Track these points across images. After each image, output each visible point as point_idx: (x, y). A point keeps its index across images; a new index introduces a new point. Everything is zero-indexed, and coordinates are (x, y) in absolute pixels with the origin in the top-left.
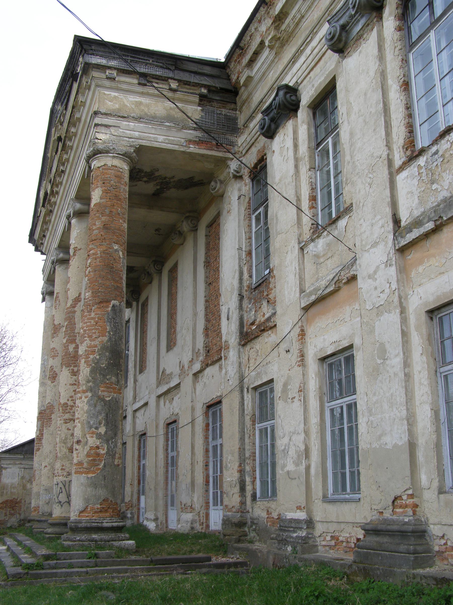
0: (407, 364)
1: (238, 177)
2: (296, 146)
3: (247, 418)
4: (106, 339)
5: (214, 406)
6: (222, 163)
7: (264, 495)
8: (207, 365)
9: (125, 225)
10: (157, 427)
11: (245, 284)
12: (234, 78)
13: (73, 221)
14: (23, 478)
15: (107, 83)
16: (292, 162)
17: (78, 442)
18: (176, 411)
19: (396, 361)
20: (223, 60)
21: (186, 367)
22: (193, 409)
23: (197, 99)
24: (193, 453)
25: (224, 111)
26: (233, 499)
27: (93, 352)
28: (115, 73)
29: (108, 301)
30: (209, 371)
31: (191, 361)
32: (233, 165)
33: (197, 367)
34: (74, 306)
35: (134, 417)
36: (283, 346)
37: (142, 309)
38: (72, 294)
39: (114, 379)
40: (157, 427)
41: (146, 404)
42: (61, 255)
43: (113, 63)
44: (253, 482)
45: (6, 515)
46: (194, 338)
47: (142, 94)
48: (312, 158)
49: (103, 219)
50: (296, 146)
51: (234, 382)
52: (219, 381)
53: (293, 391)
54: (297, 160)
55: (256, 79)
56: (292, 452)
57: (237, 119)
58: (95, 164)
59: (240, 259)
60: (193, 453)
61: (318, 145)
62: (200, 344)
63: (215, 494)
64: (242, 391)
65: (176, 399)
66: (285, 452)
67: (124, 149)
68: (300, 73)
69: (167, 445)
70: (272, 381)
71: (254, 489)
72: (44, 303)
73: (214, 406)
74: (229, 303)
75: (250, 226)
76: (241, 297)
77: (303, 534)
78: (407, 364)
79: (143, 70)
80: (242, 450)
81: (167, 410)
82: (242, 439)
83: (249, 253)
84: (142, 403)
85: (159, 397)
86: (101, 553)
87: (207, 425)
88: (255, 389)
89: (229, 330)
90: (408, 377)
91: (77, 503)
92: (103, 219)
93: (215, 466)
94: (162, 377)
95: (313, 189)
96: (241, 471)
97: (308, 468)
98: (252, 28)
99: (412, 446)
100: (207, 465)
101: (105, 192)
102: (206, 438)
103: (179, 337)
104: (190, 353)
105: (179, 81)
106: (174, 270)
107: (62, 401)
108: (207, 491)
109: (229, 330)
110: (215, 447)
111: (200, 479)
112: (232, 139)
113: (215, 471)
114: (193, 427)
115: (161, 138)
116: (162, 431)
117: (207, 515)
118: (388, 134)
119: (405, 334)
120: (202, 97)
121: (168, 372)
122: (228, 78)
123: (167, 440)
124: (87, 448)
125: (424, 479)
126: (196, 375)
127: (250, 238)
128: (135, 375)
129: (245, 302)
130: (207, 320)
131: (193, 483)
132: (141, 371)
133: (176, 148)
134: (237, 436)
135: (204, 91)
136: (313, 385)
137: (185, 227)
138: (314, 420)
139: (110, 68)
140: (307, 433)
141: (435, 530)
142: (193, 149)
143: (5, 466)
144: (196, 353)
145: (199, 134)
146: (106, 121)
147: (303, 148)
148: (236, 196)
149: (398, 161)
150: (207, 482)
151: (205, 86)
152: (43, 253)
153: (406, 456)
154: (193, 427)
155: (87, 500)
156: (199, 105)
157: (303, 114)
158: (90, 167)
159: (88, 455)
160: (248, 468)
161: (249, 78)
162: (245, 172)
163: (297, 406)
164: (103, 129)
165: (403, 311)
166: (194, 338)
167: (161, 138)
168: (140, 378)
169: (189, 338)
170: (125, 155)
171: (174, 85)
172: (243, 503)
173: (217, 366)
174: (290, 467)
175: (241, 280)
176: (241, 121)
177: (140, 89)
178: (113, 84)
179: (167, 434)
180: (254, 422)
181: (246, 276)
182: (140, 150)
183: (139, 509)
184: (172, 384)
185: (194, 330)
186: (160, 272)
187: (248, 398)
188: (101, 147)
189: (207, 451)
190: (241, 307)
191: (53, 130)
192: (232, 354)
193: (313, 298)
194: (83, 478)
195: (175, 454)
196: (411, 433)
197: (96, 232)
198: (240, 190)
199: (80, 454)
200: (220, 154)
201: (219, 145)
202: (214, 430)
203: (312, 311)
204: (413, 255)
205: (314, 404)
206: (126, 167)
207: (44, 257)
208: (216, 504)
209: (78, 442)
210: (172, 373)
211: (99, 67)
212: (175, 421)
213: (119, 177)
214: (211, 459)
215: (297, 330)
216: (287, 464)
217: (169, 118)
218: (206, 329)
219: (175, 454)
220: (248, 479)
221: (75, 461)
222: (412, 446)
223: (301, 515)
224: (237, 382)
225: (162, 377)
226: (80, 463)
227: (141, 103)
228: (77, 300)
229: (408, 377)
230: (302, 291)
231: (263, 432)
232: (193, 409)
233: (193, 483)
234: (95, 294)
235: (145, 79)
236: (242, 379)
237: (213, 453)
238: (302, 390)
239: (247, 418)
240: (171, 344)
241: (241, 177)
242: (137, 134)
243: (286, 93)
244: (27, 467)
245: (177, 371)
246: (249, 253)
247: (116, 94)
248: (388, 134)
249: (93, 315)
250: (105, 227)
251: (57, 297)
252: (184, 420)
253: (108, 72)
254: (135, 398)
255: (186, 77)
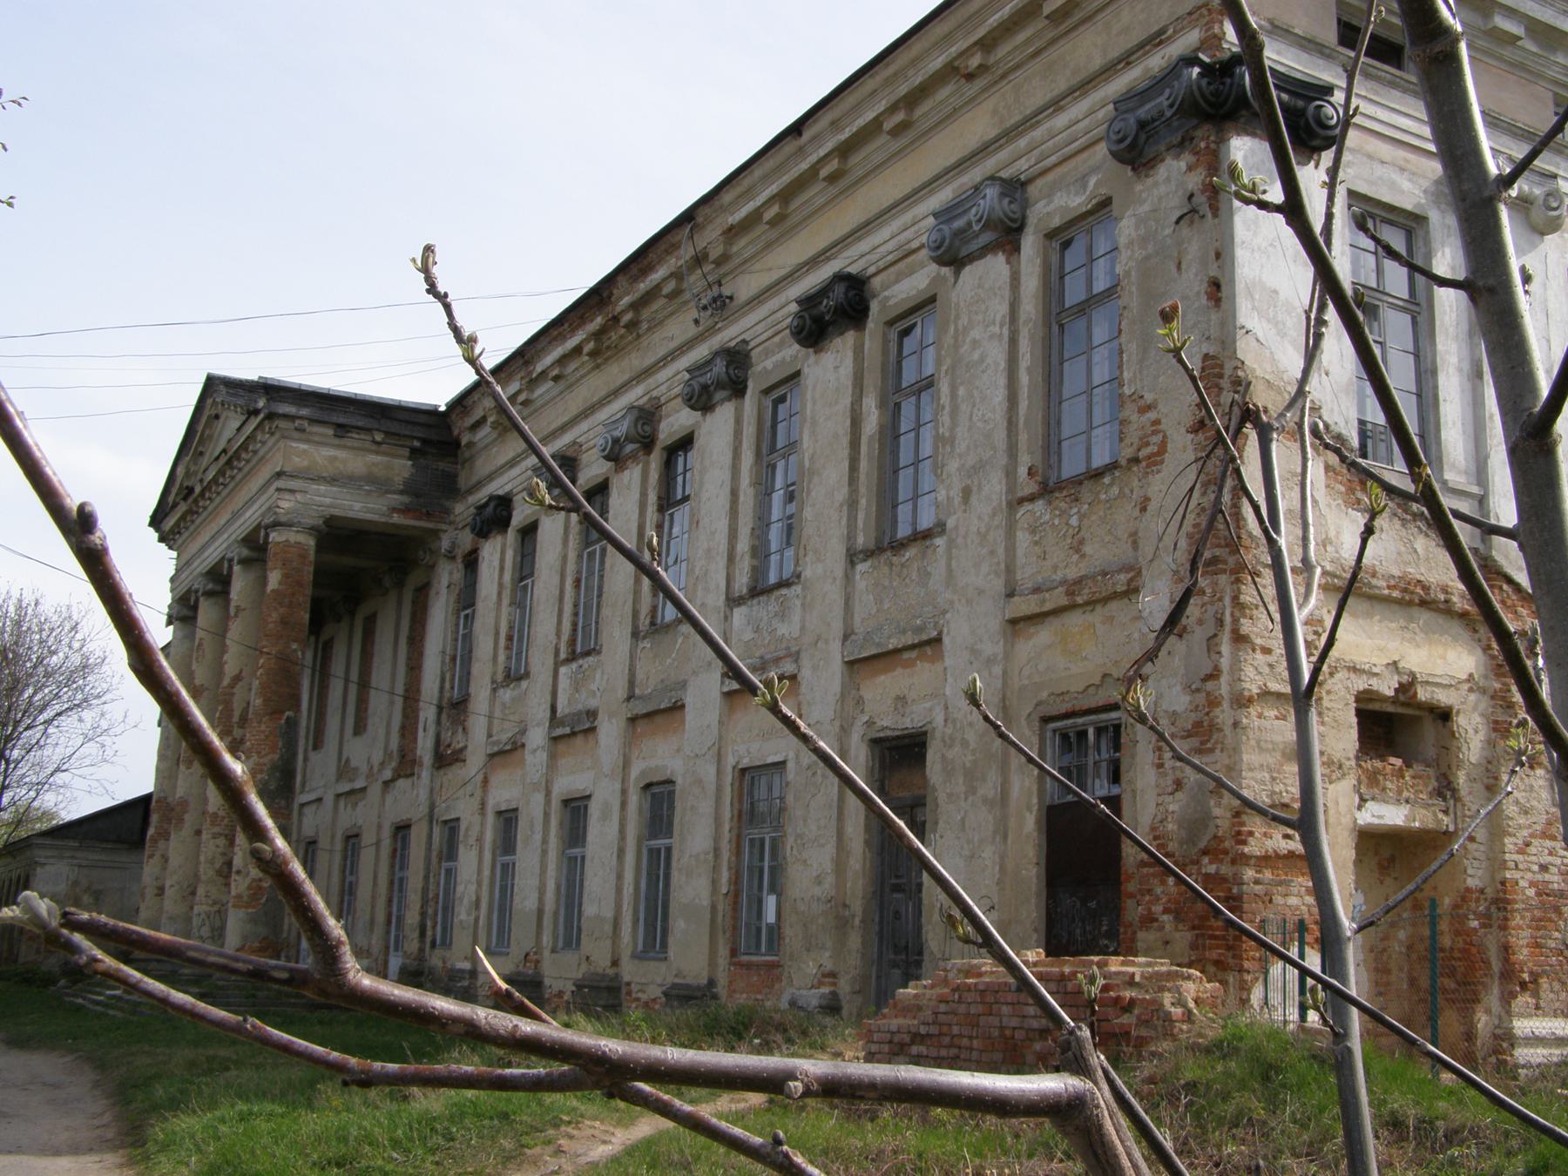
0: (545, 841)
1: (451, 557)
2: (502, 569)
3: (434, 854)
4: (277, 757)
5: (402, 829)
6: (436, 534)
7: (443, 943)
8: (399, 776)
9: (307, 616)
10: (333, 837)
11: (447, 695)
12: (456, 433)
13: (236, 568)
14: (76, 883)
15: (296, 435)
16: (495, 586)
17: (238, 872)
18: (360, 822)
19: (538, 837)
20: (443, 408)
21: (375, 769)
22: (380, 826)
23: (406, 452)
24: (375, 884)
25: (442, 465)
26: (412, 946)
27: (261, 771)
28: (306, 423)
29: (282, 712)
30: (401, 783)
31: (382, 764)
32: (445, 544)
33: (388, 774)
34: (232, 685)
35: (300, 814)
36: (469, 788)
37: (324, 649)
38: (230, 669)
39: (283, 803)
40: (333, 837)
41: (319, 800)
42: (210, 586)
43: (304, 412)
44: (434, 927)
45: (38, 952)
46: (388, 733)
47: (338, 447)
48: (513, 591)
49: (282, 610)
50: (502, 569)
51: (423, 810)
52: (410, 799)
53: (472, 841)
54: (501, 585)
55: (480, 445)
56: (465, 901)
57: (456, 476)
58: (274, 536)
59: (443, 662)
60: (375, 884)
61: (522, 579)
62: (394, 744)
63: (397, 937)
64: (431, 822)
65: (360, 805)
66: (461, 899)
67: (310, 522)
68: (515, 482)
69: (345, 866)
70: (458, 819)
71: (434, 935)
72: (171, 628)
73: (402, 830)
74: (428, 713)
75: (457, 625)
76: (440, 708)
77: (466, 983)
78: (545, 841)
79: (341, 420)
80: (425, 890)
81: (349, 817)
82: (426, 878)
83: (454, 659)
84: (312, 797)
85: (338, 796)
86: (260, 994)
87: (395, 851)
88: (445, 822)
89: (424, 745)
90: (544, 852)
91: (232, 940)
92: (282, 610)
93: (400, 902)
94: (345, 770)
95: (511, 628)
96: (423, 914)
97: (477, 920)
98: (476, 396)
99: (540, 912)
100: (390, 901)
101: (286, 576)
102: (392, 866)
103: (370, 722)
104: (381, 753)
105: (387, 433)
106: (371, 621)
107: (211, 808)
108: (388, 932)
109: (424, 745)
110: (401, 880)
111: (381, 917)
112: (447, 504)
113: (399, 910)
114: (378, 850)
115: (358, 506)
116: (339, 846)
117: (386, 962)
118: (559, 622)
119: (546, 815)
120: (414, 451)
121: (353, 763)
122: (449, 428)
123: (345, 858)
124: (248, 881)
125: (545, 939)
126: (387, 784)
127: (456, 640)
128: (306, 751)
129: (444, 716)
130: (405, 716)
131: (372, 922)
132: (316, 747)
133: (376, 518)
134: (422, 873)
135: (417, 444)
136: (489, 836)
137: (387, 582)
138: (486, 873)
139: (301, 418)
140: (479, 884)
141: (547, 982)
142: (396, 519)
143: (42, 860)
144: (387, 754)
145: (405, 499)
146: (292, 484)
147: (507, 576)
148: (447, 576)
149: (563, 656)
150: (389, 922)
151: (418, 438)
152: (170, 548)
153: (534, 919)
154: (378, 850)
155: (245, 938)
156: (410, 459)
157: (511, 534)
158: (267, 535)
159: (249, 888)
160: (430, 911)
161: (470, 444)
162: (459, 553)
163: (474, 853)
164: (287, 496)
165: (548, 794)
166: (388, 733)
167: (358, 506)
168: (313, 756)
169: (382, 731)
170: (312, 528)
171: (379, 437)
172: (422, 950)
173: (409, 781)
174: (463, 917)
175: (442, 688)
176: (463, 483)
177: (337, 441)
178: (303, 436)
179: (345, 850)
180: (440, 862)
181: (447, 685)
182: (331, 521)
183: (298, 951)
184: (359, 784)
185: (389, 725)
186: (352, 614)
187: (437, 830)
188: (283, 519)
189: (392, 883)
190: (438, 722)
191: (210, 401)
192: (425, 774)
193: (496, 749)
194: (241, 913)
195: (353, 878)
196: (541, 900)
197: (271, 626)
198: (451, 573)
199: (239, 885)
200: (430, 525)
201: (428, 515)
202: (403, 857)
203: (497, 759)
204: (562, 747)
205: (488, 856)
206: (312, 542)
207: (174, 554)
208: (396, 950)
209: (238, 872)
210: (356, 769)
211: (285, 416)
212: (357, 836)
213: (303, 556)
214: (396, 893)
215: (480, 777)
216: (462, 914)
217: (370, 479)
218: (403, 728)
219: (353, 878)
220: (429, 923)
221: (233, 892)
222: (540, 912)
223: (466, 965)
224: (427, 810)
225: (345, 770)
226: (239, 896)
227: (335, 458)
228: (237, 678)
229: (544, 852)
230: (490, 736)
231: (449, 872)
232: (380, 826)
233: (372, 922)
234: (266, 701)
235: (342, 430)
236: (432, 807)
237: (397, 885)
238: (480, 839)
239: (434, 854)
240: (360, 728)
241: (453, 558)
242: (328, 501)
243: (496, 507)
244: (84, 863)
245: (364, 769)
246: (454, 659)
247: (305, 447)
248: (559, 622)
249: (263, 727)
250: (284, 622)
251: (200, 644)
252: (368, 838)
253: (297, 422)
254: (303, 784)
255: (395, 427)
